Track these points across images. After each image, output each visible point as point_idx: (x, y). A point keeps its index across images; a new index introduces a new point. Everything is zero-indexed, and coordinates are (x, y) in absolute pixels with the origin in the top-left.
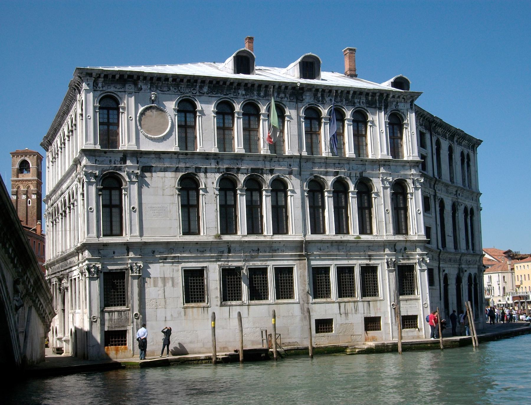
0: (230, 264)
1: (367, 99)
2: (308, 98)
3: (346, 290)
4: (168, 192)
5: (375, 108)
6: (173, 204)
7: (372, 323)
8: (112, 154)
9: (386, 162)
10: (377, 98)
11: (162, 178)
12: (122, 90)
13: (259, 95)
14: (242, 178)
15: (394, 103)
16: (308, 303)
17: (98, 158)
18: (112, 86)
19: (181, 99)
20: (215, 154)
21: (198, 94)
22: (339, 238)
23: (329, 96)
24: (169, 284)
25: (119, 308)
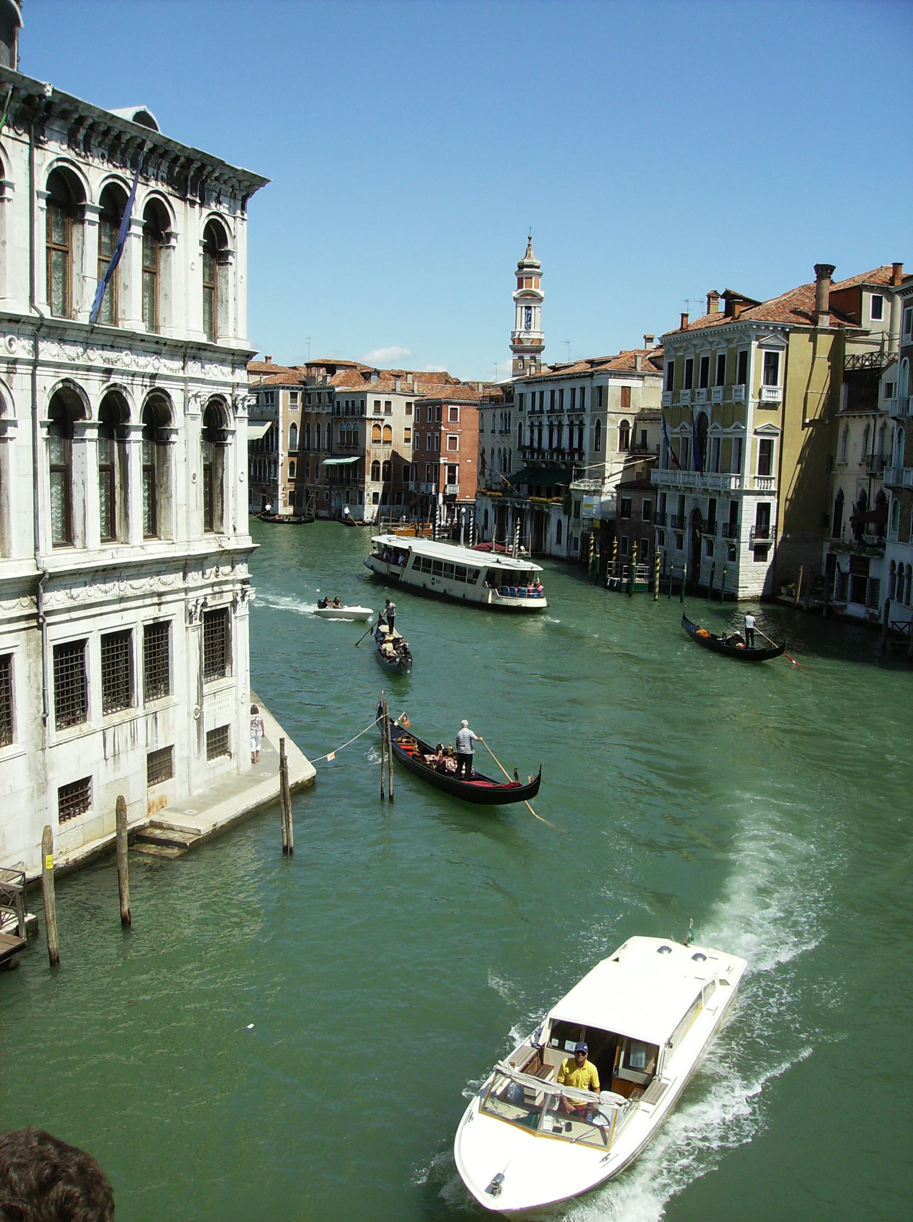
1: (170, 169)
5: (183, 199)
7: (159, 764)
9: (199, 349)
10: (192, 173)
15: (215, 195)
16: (43, 749)
23: (99, 146)
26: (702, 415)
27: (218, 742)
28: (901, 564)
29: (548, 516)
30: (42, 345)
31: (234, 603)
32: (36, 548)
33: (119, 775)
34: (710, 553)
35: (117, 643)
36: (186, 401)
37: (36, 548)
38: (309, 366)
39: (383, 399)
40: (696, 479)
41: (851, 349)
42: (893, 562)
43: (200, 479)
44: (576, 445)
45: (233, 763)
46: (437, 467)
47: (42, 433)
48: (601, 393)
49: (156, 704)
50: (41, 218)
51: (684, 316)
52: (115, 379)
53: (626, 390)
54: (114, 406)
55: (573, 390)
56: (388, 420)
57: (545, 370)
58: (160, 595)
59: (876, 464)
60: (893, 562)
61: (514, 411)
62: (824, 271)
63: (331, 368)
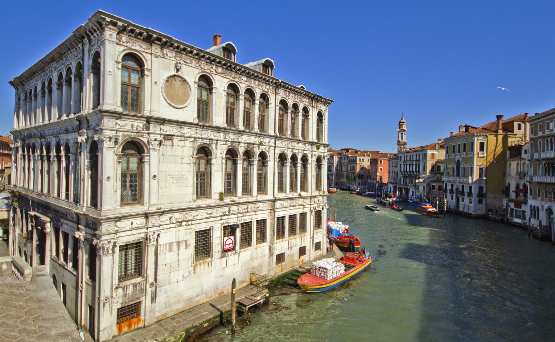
0: (230, 221)
2: (282, 92)
4: (186, 160)
6: (188, 171)
7: (302, 251)
8: (135, 118)
11: (182, 147)
12: (149, 51)
13: (255, 84)
14: (241, 150)
17: (118, 121)
18: (137, 44)
19: (201, 74)
20: (225, 129)
21: (214, 72)
22: (291, 196)
24: (183, 247)
25: (134, 281)
26: (458, 161)
27: (318, 246)
28: (534, 206)
29: (409, 190)
30: (277, 142)
31: (323, 209)
32: (274, 192)
33: (292, 253)
34: (463, 201)
35: (292, 218)
36: (312, 157)
37: (274, 192)
38: (342, 150)
39: (361, 158)
40: (457, 179)
41: (510, 140)
42: (531, 206)
43: (315, 177)
44: (417, 170)
45: (322, 252)
46: (376, 176)
47: (276, 164)
48: (425, 155)
49: (302, 235)
50: (278, 111)
51: (451, 133)
52: (295, 151)
53: (433, 155)
54: (294, 158)
55: (416, 155)
56: (363, 163)
57: (408, 149)
58: (304, 206)
59: (522, 175)
60: (531, 206)
61: (398, 161)
62: (499, 117)
63: (347, 150)
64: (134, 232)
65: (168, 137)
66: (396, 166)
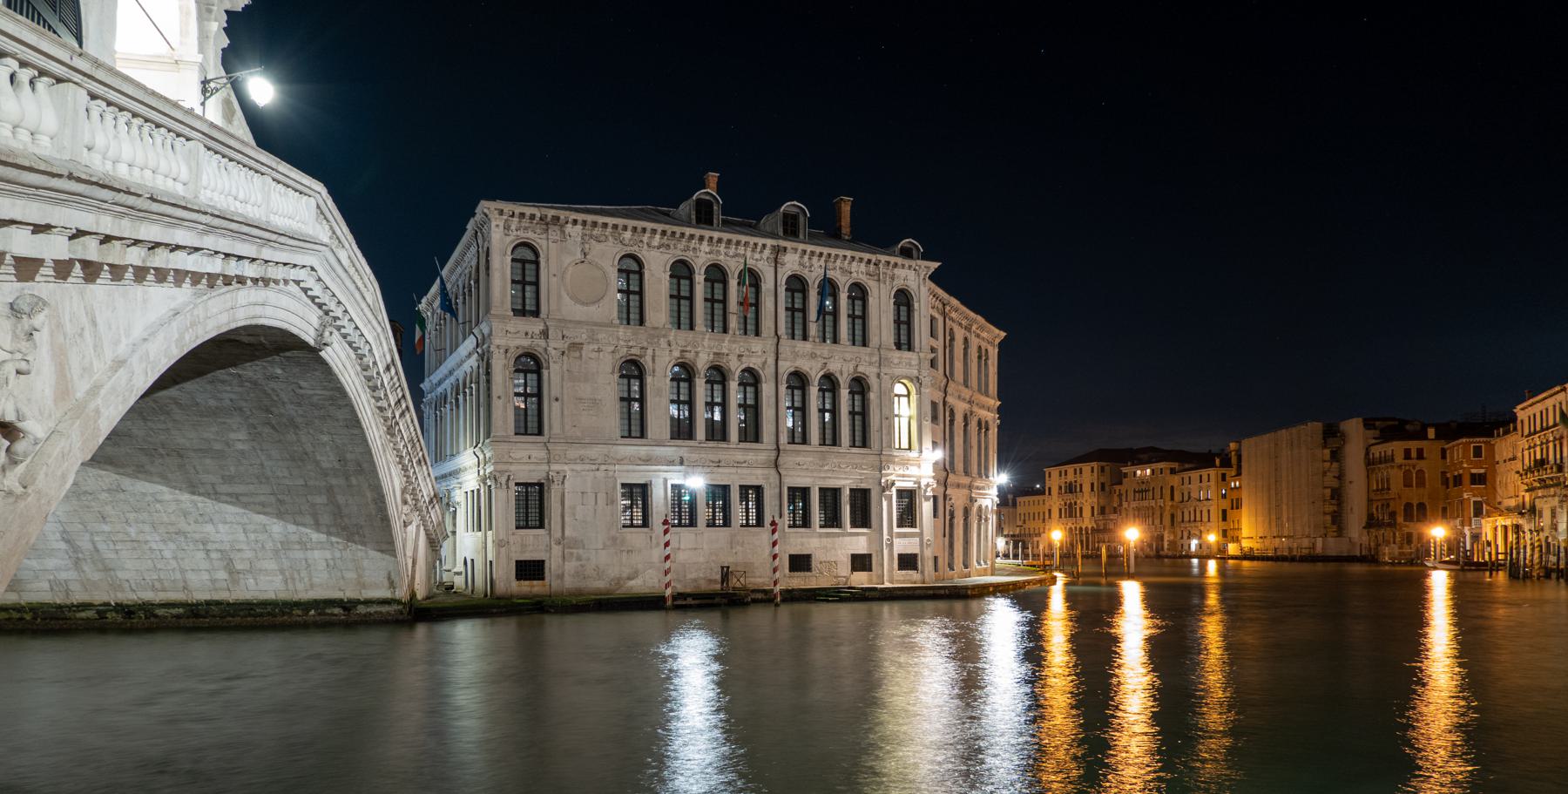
3: (832, 520)
64: (532, 467)
65: (577, 346)
66: (1514, 459)
